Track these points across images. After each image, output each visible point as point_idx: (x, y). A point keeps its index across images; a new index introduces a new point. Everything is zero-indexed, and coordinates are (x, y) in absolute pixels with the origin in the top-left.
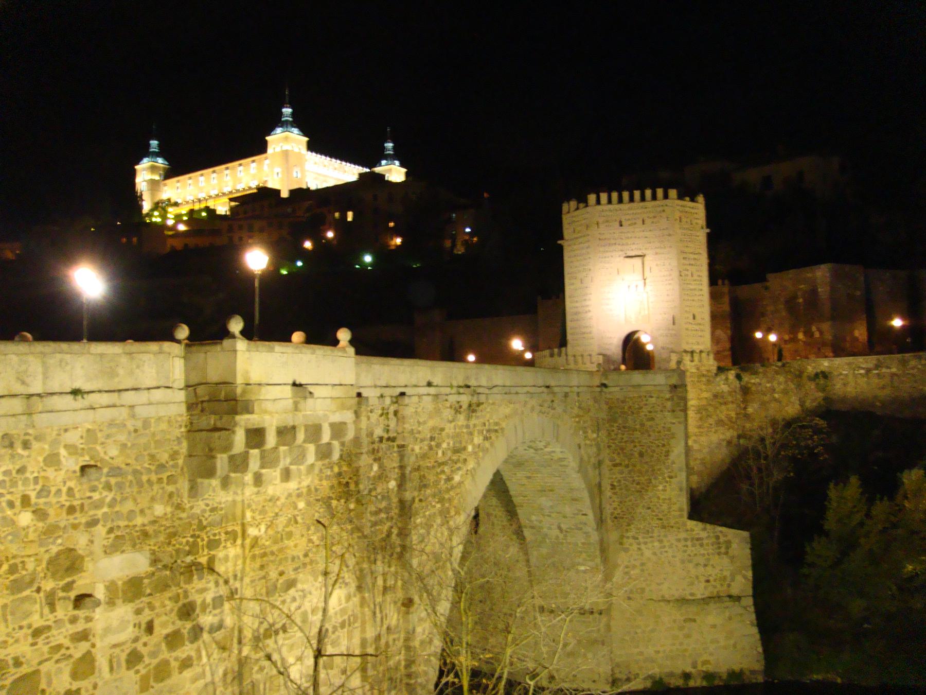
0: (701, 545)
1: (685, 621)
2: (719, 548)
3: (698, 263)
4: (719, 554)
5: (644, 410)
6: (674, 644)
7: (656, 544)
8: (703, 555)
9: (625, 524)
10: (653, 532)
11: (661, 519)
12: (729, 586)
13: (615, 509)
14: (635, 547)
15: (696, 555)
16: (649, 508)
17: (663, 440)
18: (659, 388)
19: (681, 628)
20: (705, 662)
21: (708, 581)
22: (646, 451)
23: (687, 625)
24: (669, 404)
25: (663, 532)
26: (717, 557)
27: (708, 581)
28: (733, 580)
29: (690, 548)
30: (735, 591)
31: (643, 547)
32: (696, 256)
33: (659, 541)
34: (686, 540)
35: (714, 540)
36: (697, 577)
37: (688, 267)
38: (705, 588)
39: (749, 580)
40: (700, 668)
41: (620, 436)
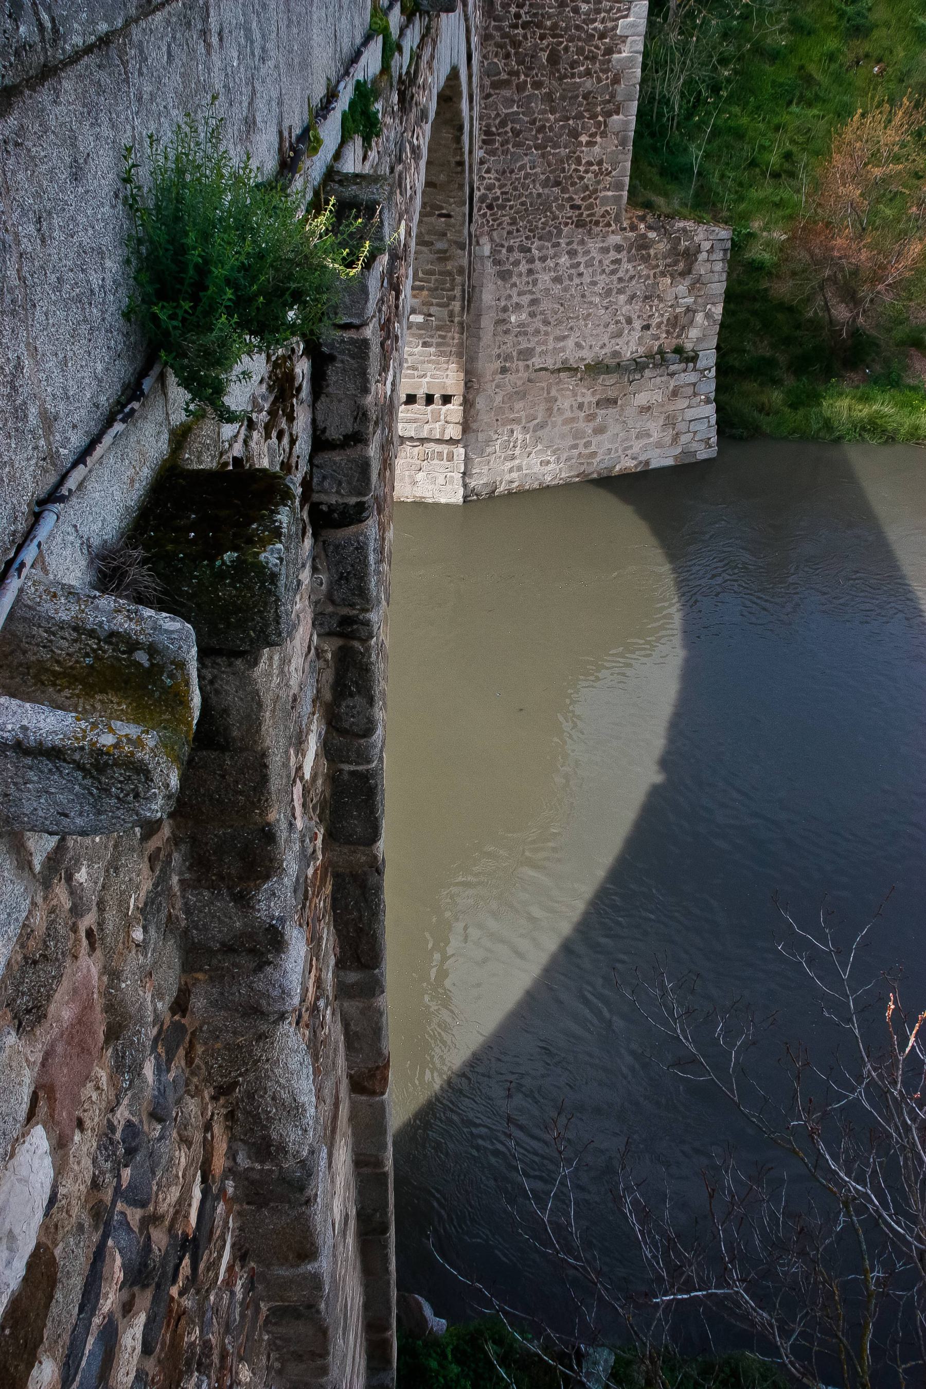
6: (575, 447)
7: (564, 260)
10: (560, 232)
11: (578, 207)
12: (679, 336)
14: (523, 267)
16: (557, 184)
19: (591, 418)
21: (647, 327)
22: (566, 49)
25: (580, 233)
29: (626, 266)
33: (568, 253)
34: (618, 248)
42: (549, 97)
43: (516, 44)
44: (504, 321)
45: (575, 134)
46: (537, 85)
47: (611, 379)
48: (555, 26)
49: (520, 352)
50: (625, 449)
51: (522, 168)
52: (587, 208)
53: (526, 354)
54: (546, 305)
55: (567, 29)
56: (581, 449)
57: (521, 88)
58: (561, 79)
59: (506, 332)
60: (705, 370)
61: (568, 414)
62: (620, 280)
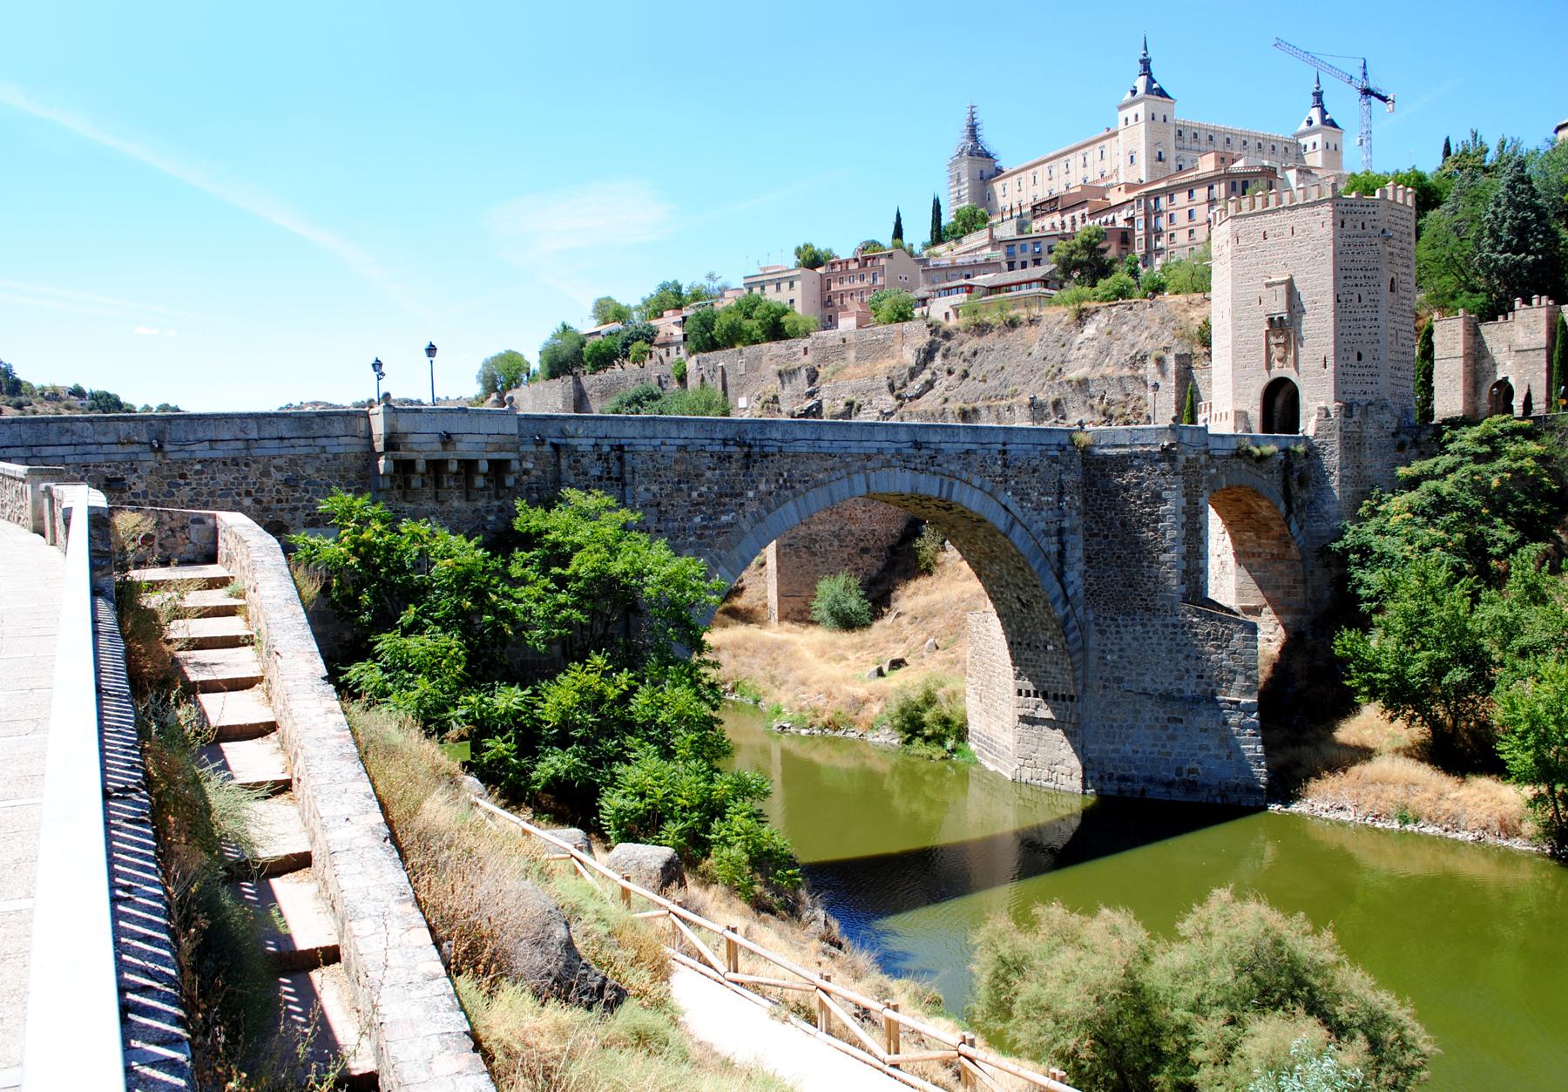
1: (1169, 719)
3: (1372, 282)
6: (1156, 745)
10: (1135, 614)
13: (1091, 585)
14: (1113, 629)
15: (1186, 645)
19: (1165, 728)
20: (1191, 771)
21: (1201, 677)
23: (1172, 726)
27: (1201, 677)
29: (1179, 637)
31: (1122, 629)
32: (1368, 274)
34: (1175, 626)
36: (1187, 671)
37: (1353, 289)
38: (1197, 684)
40: (1185, 776)
42: (1122, 543)
43: (1101, 516)
44: (1103, 658)
45: (1139, 561)
46: (1115, 536)
47: (1178, 706)
52: (1152, 601)
54: (1129, 652)
57: (1106, 537)
61: (1148, 722)
62: (1178, 644)
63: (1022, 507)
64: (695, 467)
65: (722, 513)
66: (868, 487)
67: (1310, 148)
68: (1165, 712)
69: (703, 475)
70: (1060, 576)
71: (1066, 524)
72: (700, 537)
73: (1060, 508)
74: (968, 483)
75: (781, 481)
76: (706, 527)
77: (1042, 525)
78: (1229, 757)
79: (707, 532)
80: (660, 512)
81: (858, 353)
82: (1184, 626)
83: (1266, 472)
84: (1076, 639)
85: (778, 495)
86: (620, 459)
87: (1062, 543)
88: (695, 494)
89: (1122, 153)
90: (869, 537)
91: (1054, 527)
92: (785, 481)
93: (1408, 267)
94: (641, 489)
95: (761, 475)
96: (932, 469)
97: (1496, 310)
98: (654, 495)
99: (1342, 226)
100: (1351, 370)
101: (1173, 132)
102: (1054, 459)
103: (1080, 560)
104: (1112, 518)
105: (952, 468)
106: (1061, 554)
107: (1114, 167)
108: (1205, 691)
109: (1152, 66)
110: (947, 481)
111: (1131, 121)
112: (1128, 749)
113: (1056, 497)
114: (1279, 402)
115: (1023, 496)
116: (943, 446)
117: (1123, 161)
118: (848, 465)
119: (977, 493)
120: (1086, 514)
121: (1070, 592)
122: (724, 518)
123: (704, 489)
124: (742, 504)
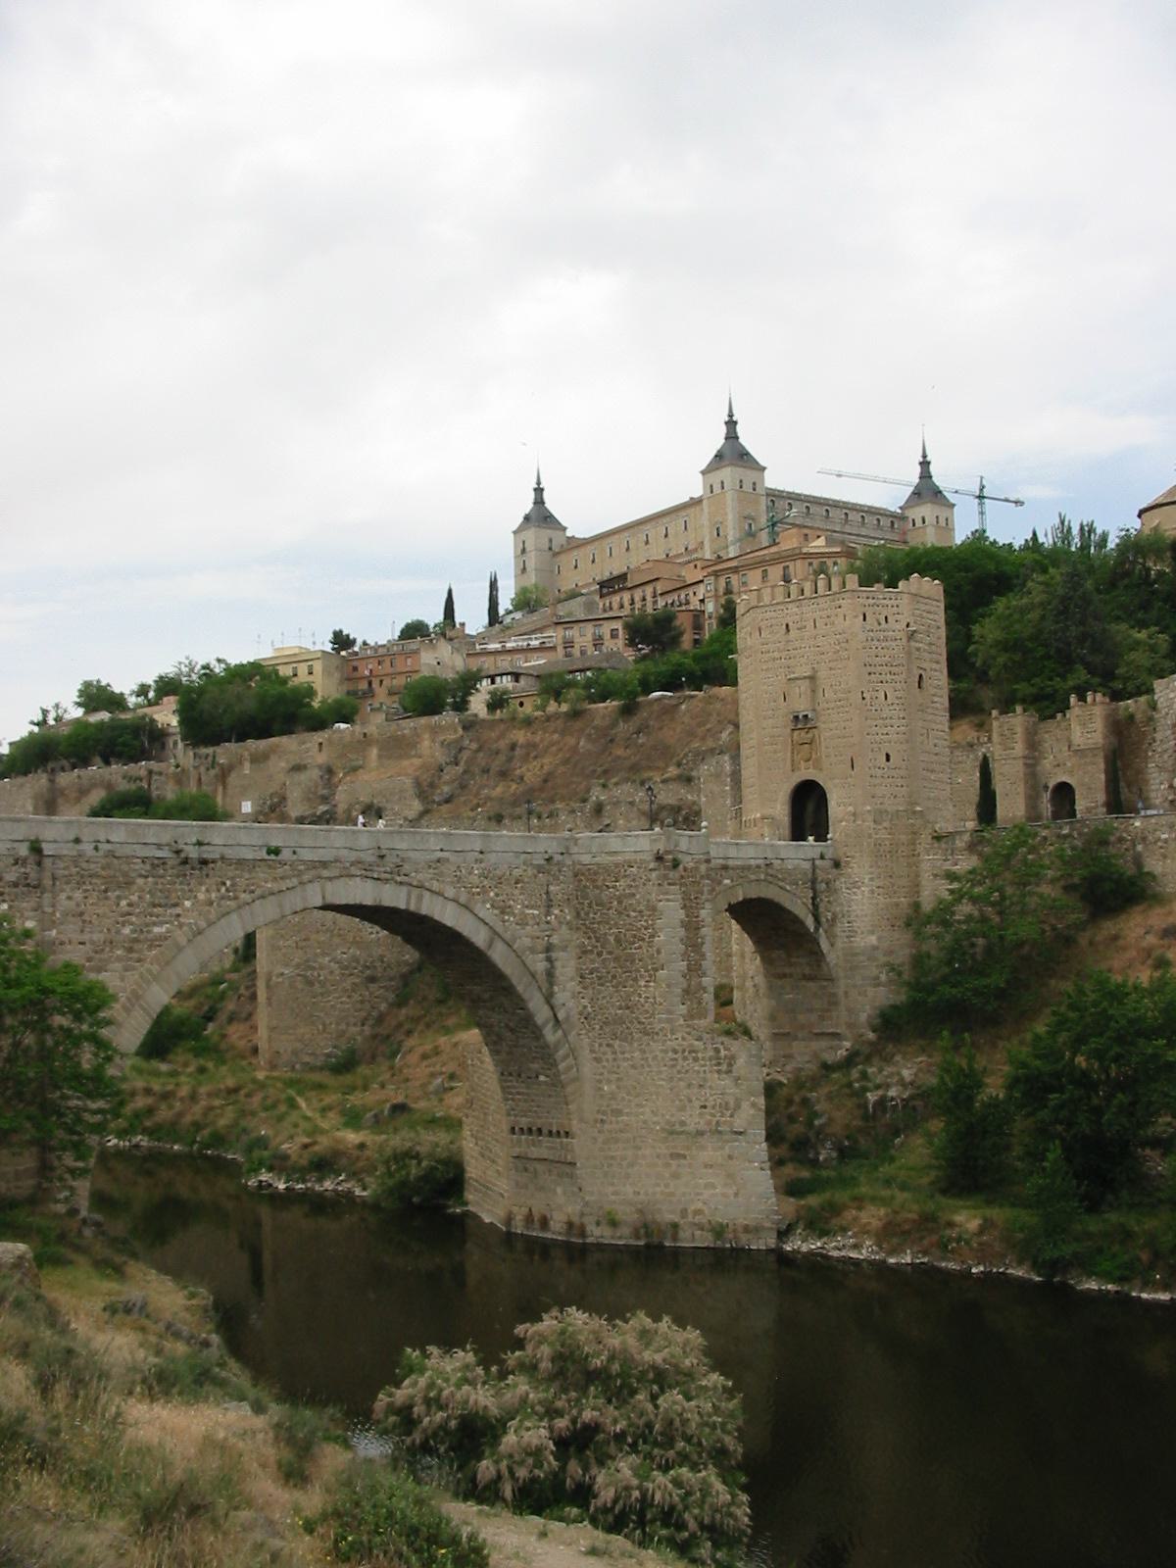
0: (696, 1059)
1: (671, 1155)
2: (719, 1064)
4: (719, 1072)
5: (622, 883)
6: (658, 1185)
7: (637, 1054)
8: (699, 1072)
9: (597, 1027)
12: (732, 1116)
14: (610, 1056)
16: (628, 1008)
17: (646, 921)
18: (639, 857)
19: (668, 1165)
20: (698, 1212)
21: (705, 1107)
23: (674, 1163)
24: (654, 875)
26: (716, 1076)
28: (738, 1106)
29: (680, 1061)
30: (739, 1123)
33: (640, 1050)
34: (675, 1052)
35: (711, 1053)
36: (690, 1101)
38: (701, 1115)
39: (760, 1110)
41: (591, 915)
44: (600, 1089)
45: (635, 980)
48: (616, 923)
49: (612, 1111)
50: (698, 1194)
51: (604, 998)
53: (618, 1112)
55: (625, 925)
56: (663, 1188)
57: (599, 954)
58: (625, 949)
59: (602, 1096)
60: (756, 1143)
62: (679, 1072)
63: (504, 922)
64: (125, 875)
65: (155, 924)
66: (324, 898)
67: (919, 523)
68: (667, 1148)
69: (133, 883)
70: (549, 998)
71: (555, 940)
72: (130, 950)
73: (548, 923)
74: (439, 894)
75: (223, 889)
76: (136, 940)
77: (527, 941)
78: (736, 1195)
79: (136, 946)
80: (84, 921)
81: (380, 750)
82: (684, 1051)
83: (791, 884)
84: (569, 1068)
85: (219, 905)
86: (39, 864)
87: (549, 960)
88: (124, 903)
89: (706, 523)
90: (378, 964)
91: (541, 944)
92: (227, 890)
93: (937, 662)
94: (63, 896)
95: (201, 884)
96: (398, 879)
97: (1049, 705)
98: (78, 905)
99: (865, 619)
100: (880, 772)
101: (763, 502)
102: (540, 869)
103: (572, 979)
104: (605, 934)
105: (420, 876)
106: (550, 974)
107: (700, 540)
108: (709, 1123)
109: (739, 428)
110: (415, 892)
111: (717, 489)
112: (629, 1190)
113: (543, 910)
114: (810, 807)
115: (504, 910)
116: (411, 854)
117: (707, 536)
118: (300, 874)
119: (451, 906)
120: (578, 929)
121: (561, 1015)
122: (156, 930)
123: (134, 898)
124: (178, 915)
